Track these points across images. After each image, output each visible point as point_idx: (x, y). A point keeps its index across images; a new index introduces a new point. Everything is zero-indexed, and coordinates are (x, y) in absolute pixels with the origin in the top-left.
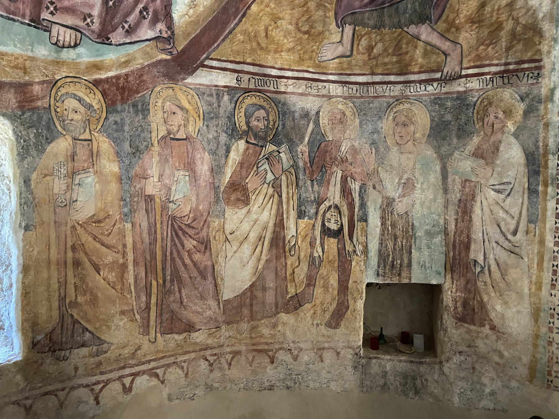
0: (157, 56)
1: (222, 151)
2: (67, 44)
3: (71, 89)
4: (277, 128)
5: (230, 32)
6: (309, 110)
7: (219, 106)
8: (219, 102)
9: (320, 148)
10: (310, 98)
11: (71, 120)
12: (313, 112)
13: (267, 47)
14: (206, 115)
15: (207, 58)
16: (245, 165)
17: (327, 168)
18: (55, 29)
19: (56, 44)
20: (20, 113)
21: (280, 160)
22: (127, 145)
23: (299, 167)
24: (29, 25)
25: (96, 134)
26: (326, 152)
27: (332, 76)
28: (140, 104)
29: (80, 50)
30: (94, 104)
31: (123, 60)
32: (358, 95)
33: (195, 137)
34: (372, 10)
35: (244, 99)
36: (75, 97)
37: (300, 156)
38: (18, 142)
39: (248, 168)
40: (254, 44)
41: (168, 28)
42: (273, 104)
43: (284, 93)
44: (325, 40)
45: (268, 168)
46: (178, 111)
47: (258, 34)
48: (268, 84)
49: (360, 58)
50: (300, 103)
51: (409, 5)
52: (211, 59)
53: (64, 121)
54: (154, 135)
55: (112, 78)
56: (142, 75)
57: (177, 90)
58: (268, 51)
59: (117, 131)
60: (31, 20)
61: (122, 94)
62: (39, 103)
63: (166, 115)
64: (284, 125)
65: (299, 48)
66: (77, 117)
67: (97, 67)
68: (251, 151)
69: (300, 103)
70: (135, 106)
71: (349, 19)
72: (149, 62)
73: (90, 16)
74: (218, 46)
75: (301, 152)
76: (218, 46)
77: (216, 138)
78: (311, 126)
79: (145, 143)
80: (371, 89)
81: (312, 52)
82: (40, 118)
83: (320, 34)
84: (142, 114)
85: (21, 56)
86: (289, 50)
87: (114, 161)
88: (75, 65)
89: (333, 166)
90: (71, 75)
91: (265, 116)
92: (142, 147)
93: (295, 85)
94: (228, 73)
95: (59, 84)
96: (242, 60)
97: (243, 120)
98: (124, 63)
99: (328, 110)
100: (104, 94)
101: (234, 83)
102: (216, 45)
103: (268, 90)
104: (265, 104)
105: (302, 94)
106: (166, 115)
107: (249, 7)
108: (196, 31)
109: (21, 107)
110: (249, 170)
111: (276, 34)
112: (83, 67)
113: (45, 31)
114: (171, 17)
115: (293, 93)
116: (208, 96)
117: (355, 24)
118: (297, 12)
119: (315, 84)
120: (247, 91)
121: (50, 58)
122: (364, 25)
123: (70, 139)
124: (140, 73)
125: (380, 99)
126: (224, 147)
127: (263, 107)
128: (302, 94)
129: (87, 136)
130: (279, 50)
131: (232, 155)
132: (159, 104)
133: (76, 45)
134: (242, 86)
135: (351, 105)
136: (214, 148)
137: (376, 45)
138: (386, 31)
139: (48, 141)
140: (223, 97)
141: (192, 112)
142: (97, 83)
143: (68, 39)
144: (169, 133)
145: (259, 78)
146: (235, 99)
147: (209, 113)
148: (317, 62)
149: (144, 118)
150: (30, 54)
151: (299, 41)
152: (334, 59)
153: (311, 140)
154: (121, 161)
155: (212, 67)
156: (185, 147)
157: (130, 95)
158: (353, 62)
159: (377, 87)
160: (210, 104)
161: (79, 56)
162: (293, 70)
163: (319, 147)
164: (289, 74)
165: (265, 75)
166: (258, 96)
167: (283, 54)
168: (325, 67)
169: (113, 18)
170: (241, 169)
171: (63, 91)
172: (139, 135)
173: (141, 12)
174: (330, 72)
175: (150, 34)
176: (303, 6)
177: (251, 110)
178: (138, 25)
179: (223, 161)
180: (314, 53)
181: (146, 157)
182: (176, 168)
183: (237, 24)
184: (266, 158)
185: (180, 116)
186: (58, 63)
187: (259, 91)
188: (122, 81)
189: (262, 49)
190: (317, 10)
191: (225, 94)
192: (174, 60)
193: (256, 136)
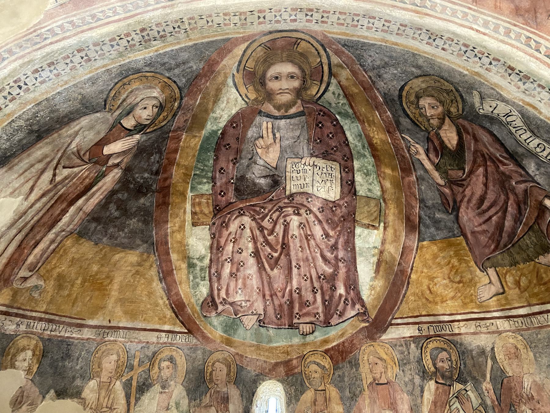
0: (360, 325)
1: (417, 391)
2: (308, 333)
3: (312, 359)
4: (460, 368)
5: (404, 297)
6: (484, 348)
7: (409, 353)
8: (409, 350)
9: (503, 385)
10: (483, 335)
11: (314, 378)
12: (489, 349)
13: (434, 301)
14: (401, 362)
15: (393, 318)
16: (438, 404)
17: (516, 407)
18: (301, 326)
19: (303, 334)
20: (286, 378)
21: (468, 398)
22: (347, 393)
23: (487, 405)
24: (288, 328)
25: (328, 386)
26: (511, 389)
27: (496, 313)
28: (353, 361)
29: (316, 334)
30: (326, 366)
31: (340, 333)
32: (524, 327)
33: (394, 381)
34: (502, 253)
35: (427, 344)
36: (315, 363)
37: (486, 394)
38: (286, 396)
39: (441, 406)
40: (424, 300)
41: (362, 306)
42: (453, 346)
43: (459, 334)
44: (478, 284)
45: (459, 407)
46: (379, 362)
47: (424, 292)
48: (445, 328)
49: (513, 293)
50: (474, 341)
51: (528, 241)
52: (396, 319)
53: (310, 379)
54: (364, 382)
55: (335, 346)
56: (353, 340)
57: (376, 346)
58: (436, 303)
59: (340, 382)
60: (289, 326)
61: (342, 356)
62: (296, 371)
63: (371, 366)
64: (465, 364)
65: (459, 295)
66: (317, 375)
67: (326, 341)
68: (441, 391)
69: (474, 341)
70: (350, 362)
71: (487, 264)
72: (356, 331)
73: (318, 313)
74: (398, 308)
75: (486, 390)
76: (398, 308)
77: (412, 380)
78: (490, 362)
79: (359, 389)
80: (534, 319)
81: (472, 295)
82: (297, 380)
83: (471, 280)
84: (356, 368)
85: (286, 345)
86: (453, 298)
87: (339, 404)
88: (314, 343)
89: (521, 404)
90: (312, 350)
91: (448, 356)
92: (357, 392)
93: (466, 326)
94: (411, 326)
95: (306, 357)
96: (418, 314)
97: (430, 362)
98: (341, 335)
99: (501, 345)
100: (331, 358)
101: (417, 333)
102: (396, 308)
103: (445, 334)
104: (445, 346)
105: (474, 334)
106: (371, 366)
107: (410, 277)
108: (380, 302)
109: (287, 375)
110: (443, 409)
111: (439, 289)
112: (318, 344)
113: (296, 329)
114: (362, 300)
115: (467, 334)
116: (399, 346)
117: (494, 266)
118: (446, 270)
119: (482, 323)
120: (428, 337)
121: (301, 343)
122: (502, 266)
123: (313, 391)
124: (351, 340)
125: (545, 329)
126: (419, 388)
127: (444, 349)
128: (474, 334)
129: (322, 388)
130: (444, 299)
131: (426, 394)
132: (366, 358)
133: (313, 332)
134: (423, 334)
135: (521, 338)
136: (411, 389)
137: (520, 279)
138: (521, 266)
139: (302, 393)
140: (410, 345)
141: (389, 361)
142: (326, 352)
143: (308, 330)
144: (375, 380)
145: (436, 325)
146: (421, 345)
147: (402, 360)
148: (479, 303)
149: (357, 370)
150: (290, 344)
151: (458, 290)
152: (491, 298)
153: (492, 377)
154: (344, 404)
155: (398, 324)
156: (388, 390)
157: (346, 356)
158: (509, 297)
159: (539, 318)
160: (402, 353)
161: (315, 337)
162: (460, 314)
163: (502, 383)
164: (459, 317)
165: (440, 322)
166: (439, 340)
167: (448, 302)
168: (488, 306)
169: (329, 311)
170: (436, 408)
171: (308, 360)
172: (355, 383)
173: (344, 302)
174: (493, 309)
175: (353, 313)
176: (449, 264)
177: (435, 352)
178: (344, 309)
179: (419, 401)
180: (473, 296)
181: (360, 400)
182: (382, 408)
183: (407, 290)
184: (456, 397)
185: (381, 366)
186: (305, 344)
187: (439, 336)
188: (341, 347)
189: (430, 302)
190: (460, 264)
191: (412, 342)
192: (372, 324)
193: (443, 377)
